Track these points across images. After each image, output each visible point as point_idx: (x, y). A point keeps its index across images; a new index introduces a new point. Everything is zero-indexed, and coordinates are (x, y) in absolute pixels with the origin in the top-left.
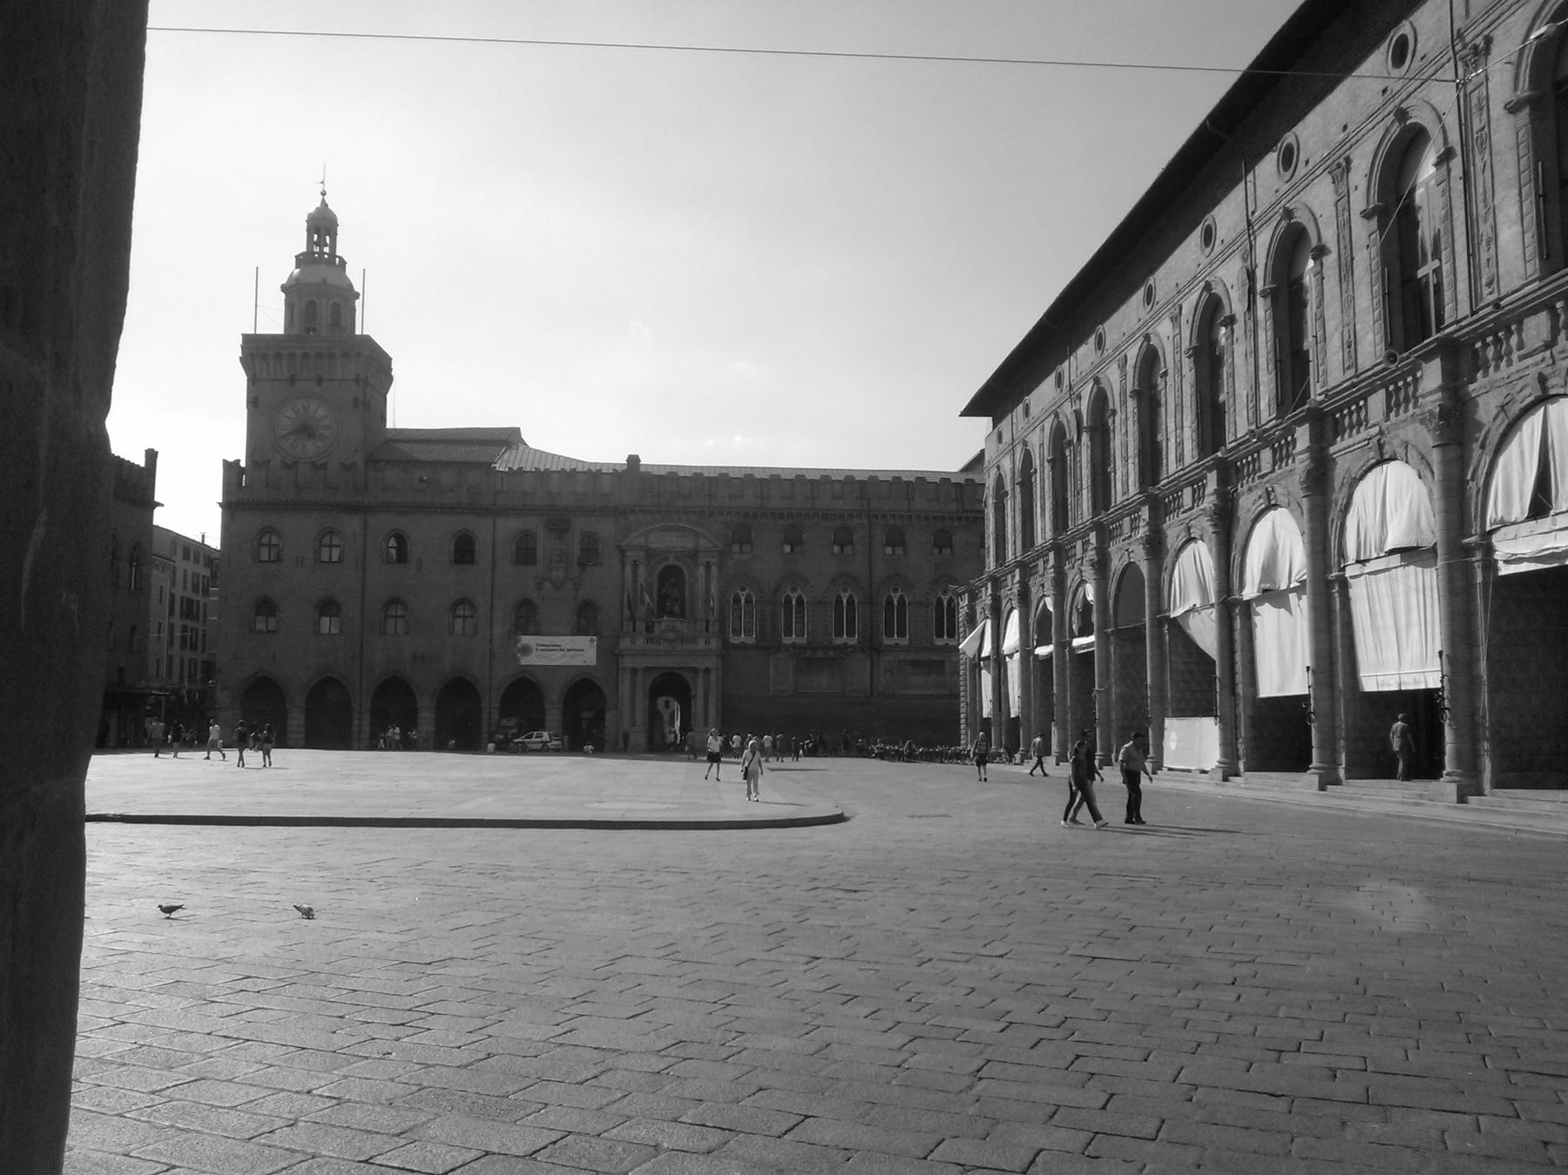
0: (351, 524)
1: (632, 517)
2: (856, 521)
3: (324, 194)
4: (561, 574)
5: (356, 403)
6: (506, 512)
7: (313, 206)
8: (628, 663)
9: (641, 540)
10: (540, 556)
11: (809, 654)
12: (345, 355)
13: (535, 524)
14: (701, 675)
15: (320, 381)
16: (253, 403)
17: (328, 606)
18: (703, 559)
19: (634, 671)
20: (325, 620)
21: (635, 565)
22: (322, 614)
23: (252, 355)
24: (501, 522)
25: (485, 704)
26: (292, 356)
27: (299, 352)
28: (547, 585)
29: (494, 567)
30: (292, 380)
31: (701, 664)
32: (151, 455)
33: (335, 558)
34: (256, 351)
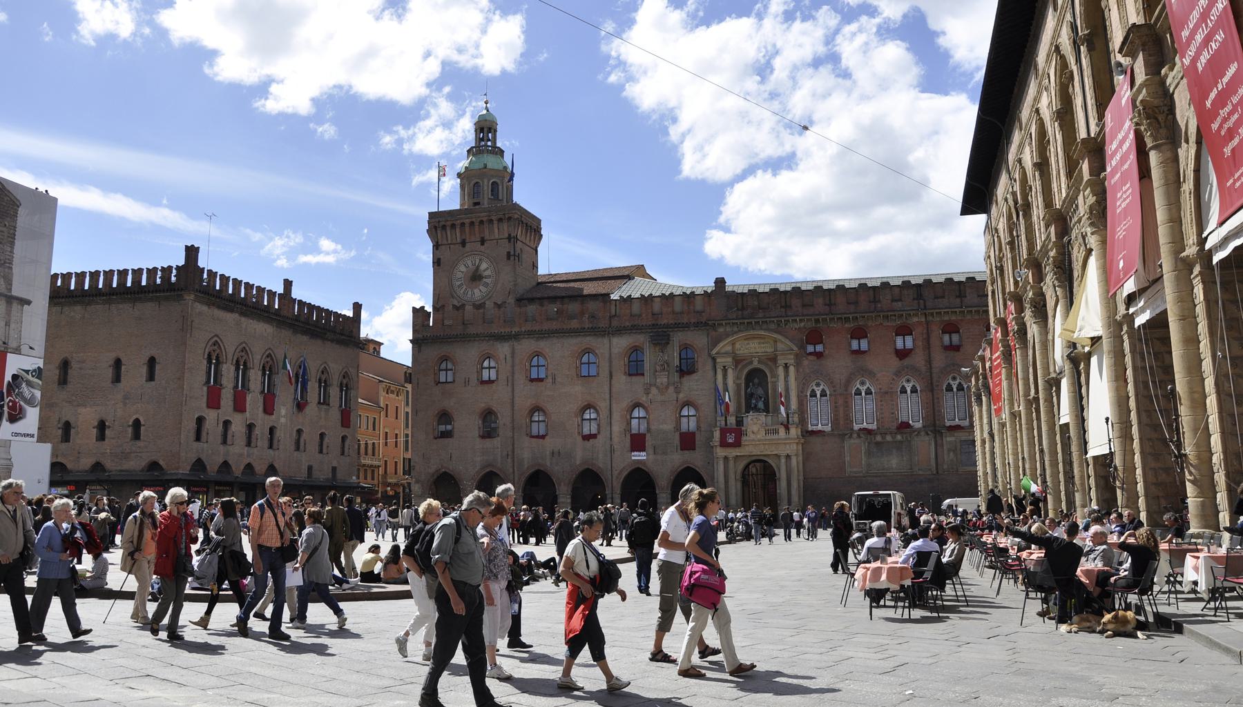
0: (503, 349)
6: (620, 331)
9: (729, 348)
10: (647, 366)
11: (879, 438)
12: (500, 220)
15: (483, 242)
16: (437, 263)
18: (781, 361)
19: (726, 458)
21: (725, 370)
24: (615, 340)
27: (467, 221)
30: (463, 243)
31: (783, 451)
32: (357, 307)
34: (439, 224)
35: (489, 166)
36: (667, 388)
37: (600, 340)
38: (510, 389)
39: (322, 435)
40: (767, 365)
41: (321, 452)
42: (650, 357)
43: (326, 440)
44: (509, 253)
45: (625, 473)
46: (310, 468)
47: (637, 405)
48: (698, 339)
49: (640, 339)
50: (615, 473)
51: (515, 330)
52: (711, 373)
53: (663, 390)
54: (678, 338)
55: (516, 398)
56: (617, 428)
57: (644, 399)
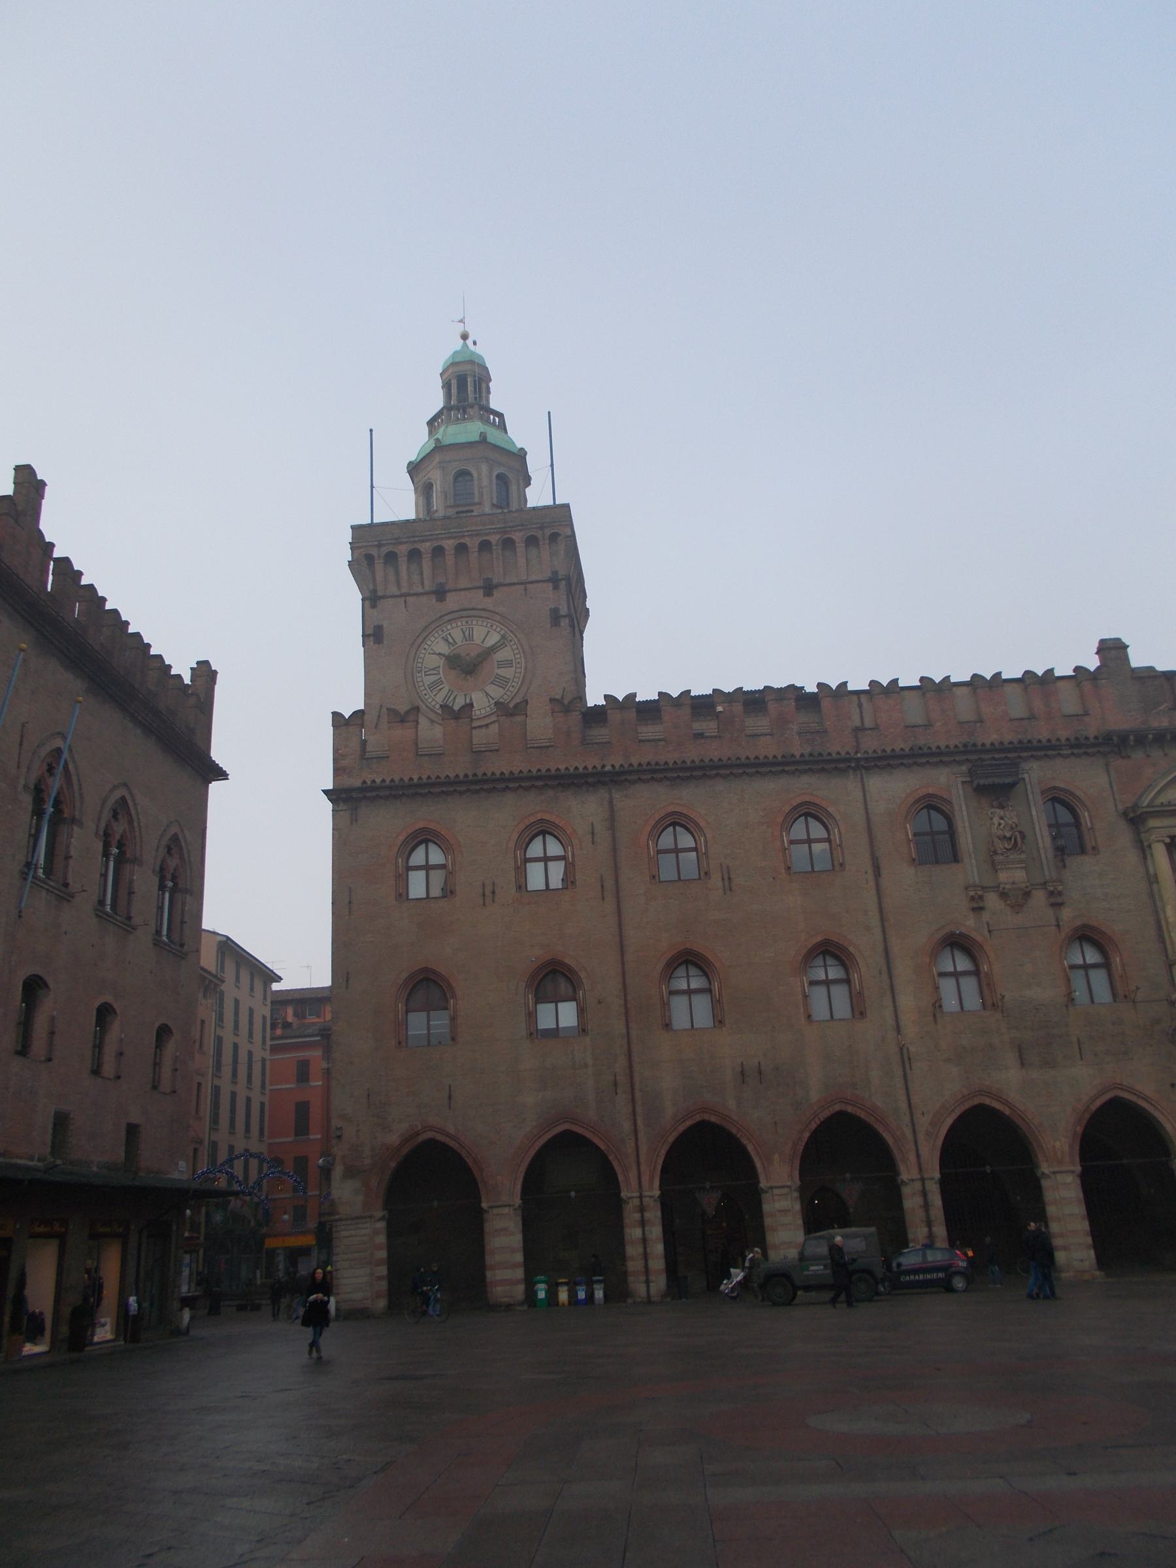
0: (584, 811)
1: (1138, 755)
3: (465, 337)
4: (1019, 875)
5: (556, 617)
6: (885, 762)
7: (448, 347)
10: (965, 841)
12: (532, 541)
15: (489, 589)
16: (373, 636)
17: (552, 978)
22: (539, 1000)
23: (370, 559)
25: (907, 1173)
26: (439, 551)
27: (449, 544)
28: (992, 901)
30: (440, 593)
33: (556, 882)
34: (377, 554)
35: (490, 439)
36: (1027, 894)
39: (104, 1013)
41: (96, 1072)
42: (974, 824)
43: (115, 1031)
45: (949, 1121)
46: (61, 1121)
47: (957, 942)
48: (1089, 780)
49: (946, 781)
50: (923, 1122)
51: (614, 761)
52: (1132, 857)
53: (1017, 899)
56: (907, 1001)
57: (969, 924)
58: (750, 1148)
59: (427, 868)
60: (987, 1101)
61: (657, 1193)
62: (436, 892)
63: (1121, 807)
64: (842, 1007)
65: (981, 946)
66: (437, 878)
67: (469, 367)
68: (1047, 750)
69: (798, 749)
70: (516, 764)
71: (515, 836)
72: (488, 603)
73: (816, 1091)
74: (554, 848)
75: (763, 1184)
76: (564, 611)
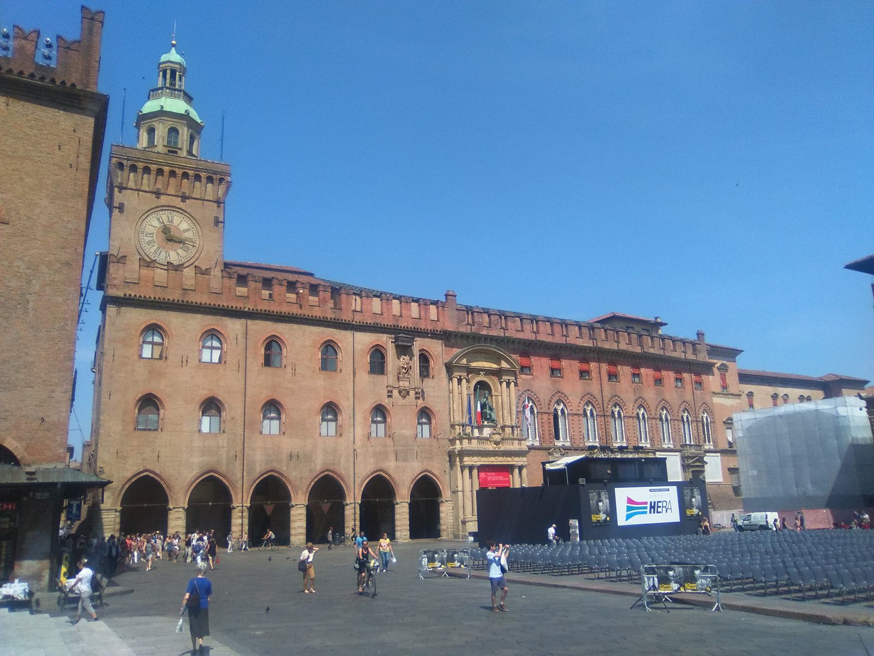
0: (233, 327)
2: (591, 355)
5: (217, 222)
8: (468, 461)
13: (386, 341)
14: (516, 471)
15: (184, 198)
17: (211, 406)
19: (471, 468)
20: (206, 420)
25: (349, 500)
28: (395, 393)
29: (354, 373)
30: (158, 194)
33: (216, 359)
37: (343, 332)
38: (241, 374)
40: (491, 379)
42: (392, 361)
44: (216, 218)
48: (435, 347)
50: (358, 481)
53: (404, 393)
54: (418, 344)
55: (249, 388)
56: (359, 431)
57: (386, 402)
58: (290, 488)
59: (153, 343)
60: (381, 473)
61: (249, 505)
62: (157, 356)
63: (445, 361)
64: (332, 432)
65: (388, 411)
66: (158, 350)
67: (178, 66)
68: (423, 334)
69: (330, 315)
70: (202, 299)
71: (200, 335)
72: (182, 205)
73: (319, 465)
74: (216, 344)
75: (293, 503)
76: (221, 219)
